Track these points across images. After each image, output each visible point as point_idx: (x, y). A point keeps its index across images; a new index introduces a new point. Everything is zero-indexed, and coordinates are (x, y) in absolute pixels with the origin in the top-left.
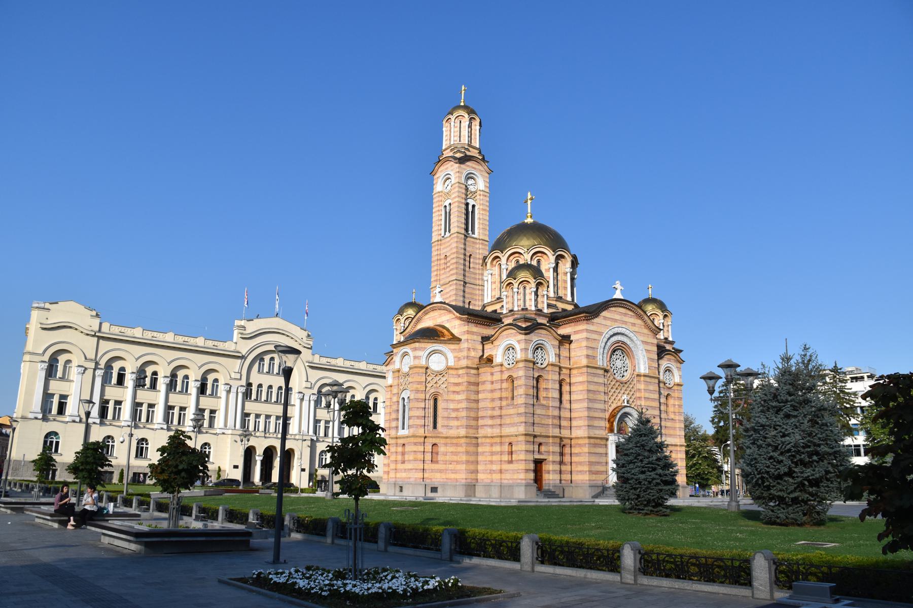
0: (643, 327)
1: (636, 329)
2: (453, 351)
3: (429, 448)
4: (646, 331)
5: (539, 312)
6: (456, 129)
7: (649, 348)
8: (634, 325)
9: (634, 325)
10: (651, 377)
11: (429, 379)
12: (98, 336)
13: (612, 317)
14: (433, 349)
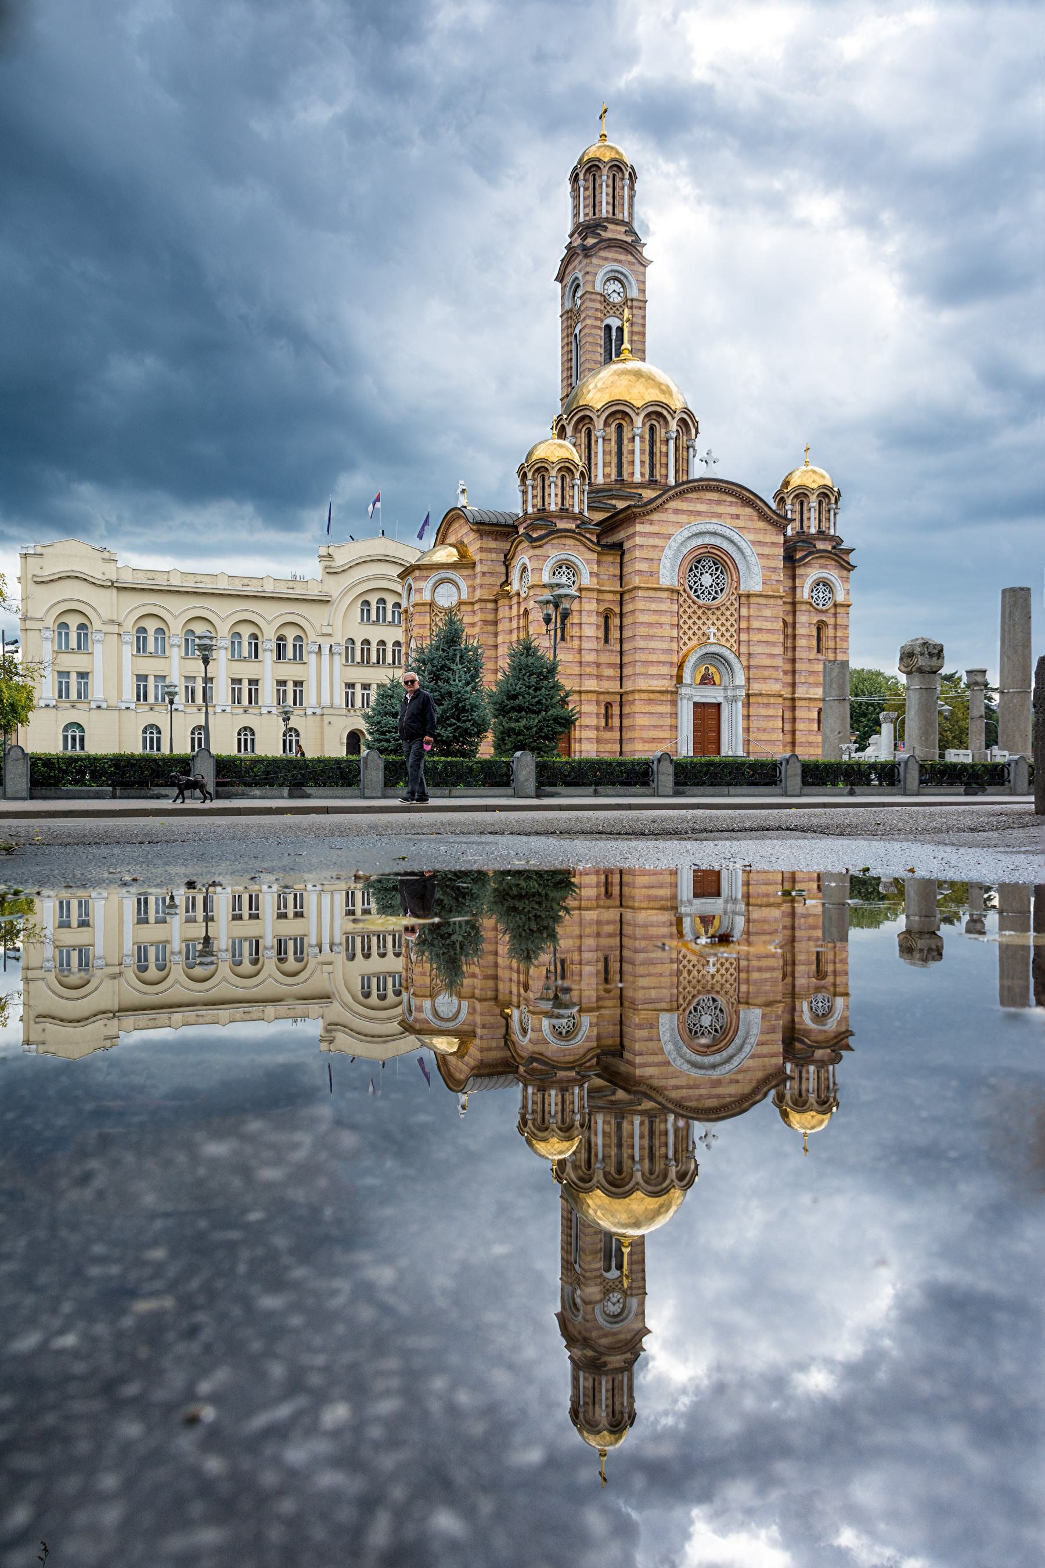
1: (740, 523)
2: (465, 577)
4: (761, 525)
5: (564, 512)
7: (766, 551)
8: (738, 517)
9: (738, 517)
12: (117, 587)
13: (691, 508)
14: (438, 577)
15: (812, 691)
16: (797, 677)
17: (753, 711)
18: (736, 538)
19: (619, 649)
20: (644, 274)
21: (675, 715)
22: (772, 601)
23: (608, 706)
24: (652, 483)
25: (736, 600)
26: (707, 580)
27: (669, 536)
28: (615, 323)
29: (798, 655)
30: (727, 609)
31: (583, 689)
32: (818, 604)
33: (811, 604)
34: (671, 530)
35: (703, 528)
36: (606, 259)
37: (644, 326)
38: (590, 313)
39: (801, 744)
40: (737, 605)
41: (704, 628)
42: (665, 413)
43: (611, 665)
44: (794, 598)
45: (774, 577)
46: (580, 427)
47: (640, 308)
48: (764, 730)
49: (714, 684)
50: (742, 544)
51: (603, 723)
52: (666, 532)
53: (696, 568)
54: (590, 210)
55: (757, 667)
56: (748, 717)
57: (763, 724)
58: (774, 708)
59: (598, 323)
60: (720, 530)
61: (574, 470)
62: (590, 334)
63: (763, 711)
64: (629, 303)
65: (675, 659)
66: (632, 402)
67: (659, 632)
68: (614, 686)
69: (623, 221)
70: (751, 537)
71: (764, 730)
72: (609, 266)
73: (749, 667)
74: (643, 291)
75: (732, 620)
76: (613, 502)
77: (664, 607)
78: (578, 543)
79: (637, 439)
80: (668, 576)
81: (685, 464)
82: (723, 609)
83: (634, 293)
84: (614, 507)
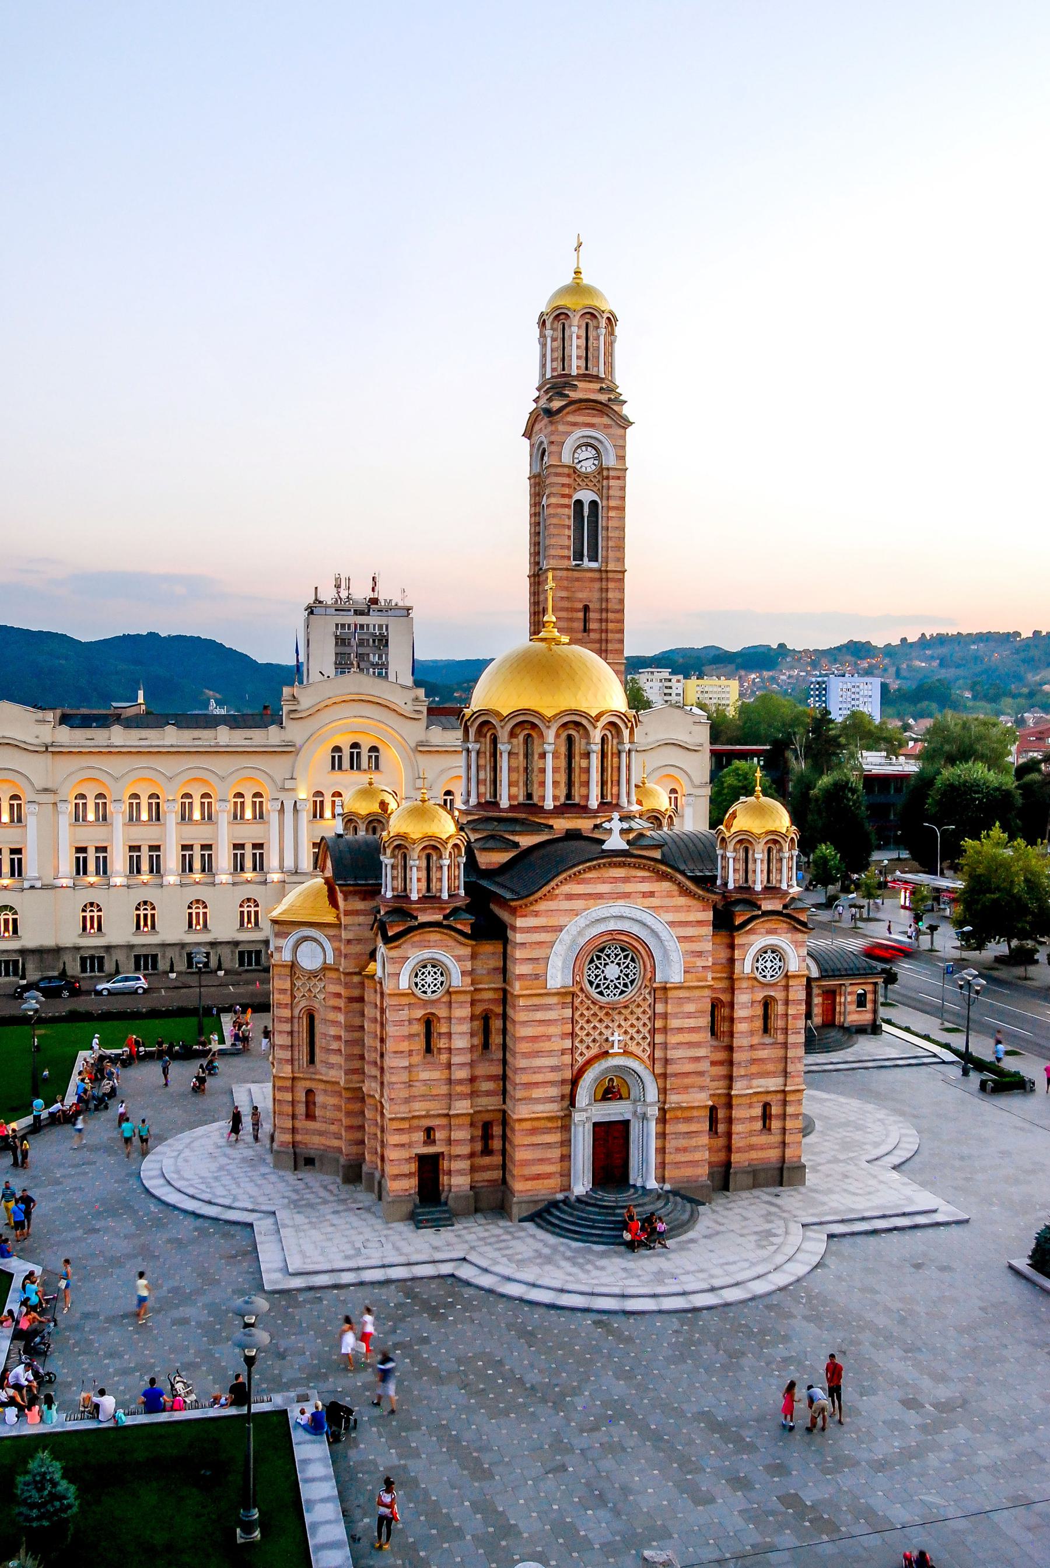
0: (676, 893)
1: (654, 902)
3: (301, 1096)
4: (682, 901)
6: (555, 344)
7: (690, 931)
8: (651, 894)
9: (651, 894)
10: (689, 988)
11: (298, 983)
15: (755, 1082)
16: (735, 1069)
17: (669, 1129)
18: (649, 920)
19: (501, 1056)
20: (623, 437)
21: (566, 1143)
22: (697, 993)
23: (487, 1126)
24: (569, 807)
25: (650, 993)
26: (612, 971)
27: (560, 929)
28: (586, 496)
29: (736, 1042)
30: (639, 1006)
31: (452, 1113)
32: (764, 976)
33: (755, 979)
34: (562, 920)
35: (605, 913)
36: (575, 424)
37: (623, 498)
38: (554, 490)
39: (739, 1150)
40: (651, 1000)
41: (607, 1033)
42: (584, 722)
43: (490, 1078)
44: (733, 973)
45: (700, 963)
46: (485, 730)
47: (618, 478)
48: (685, 1150)
49: (621, 1098)
50: (658, 927)
51: (478, 1146)
52: (556, 924)
53: (599, 958)
54: (558, 365)
55: (676, 1075)
56: (662, 1135)
57: (682, 1143)
58: (698, 1122)
59: (565, 501)
60: (627, 912)
61: (442, 849)
62: (554, 515)
63: (683, 1128)
64: (605, 473)
65: (568, 1075)
66: (541, 710)
67: (546, 1046)
68: (492, 1103)
69: (597, 377)
70: (670, 917)
71: (685, 1150)
72: (579, 433)
73: (665, 1076)
74: (622, 458)
75: (645, 1019)
76: (516, 839)
77: (552, 1015)
78: (445, 937)
79: (549, 756)
80: (558, 977)
81: (615, 774)
82: (633, 1006)
83: (610, 460)
84: (516, 845)
